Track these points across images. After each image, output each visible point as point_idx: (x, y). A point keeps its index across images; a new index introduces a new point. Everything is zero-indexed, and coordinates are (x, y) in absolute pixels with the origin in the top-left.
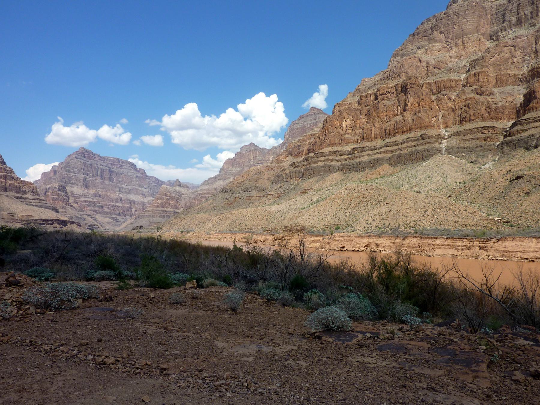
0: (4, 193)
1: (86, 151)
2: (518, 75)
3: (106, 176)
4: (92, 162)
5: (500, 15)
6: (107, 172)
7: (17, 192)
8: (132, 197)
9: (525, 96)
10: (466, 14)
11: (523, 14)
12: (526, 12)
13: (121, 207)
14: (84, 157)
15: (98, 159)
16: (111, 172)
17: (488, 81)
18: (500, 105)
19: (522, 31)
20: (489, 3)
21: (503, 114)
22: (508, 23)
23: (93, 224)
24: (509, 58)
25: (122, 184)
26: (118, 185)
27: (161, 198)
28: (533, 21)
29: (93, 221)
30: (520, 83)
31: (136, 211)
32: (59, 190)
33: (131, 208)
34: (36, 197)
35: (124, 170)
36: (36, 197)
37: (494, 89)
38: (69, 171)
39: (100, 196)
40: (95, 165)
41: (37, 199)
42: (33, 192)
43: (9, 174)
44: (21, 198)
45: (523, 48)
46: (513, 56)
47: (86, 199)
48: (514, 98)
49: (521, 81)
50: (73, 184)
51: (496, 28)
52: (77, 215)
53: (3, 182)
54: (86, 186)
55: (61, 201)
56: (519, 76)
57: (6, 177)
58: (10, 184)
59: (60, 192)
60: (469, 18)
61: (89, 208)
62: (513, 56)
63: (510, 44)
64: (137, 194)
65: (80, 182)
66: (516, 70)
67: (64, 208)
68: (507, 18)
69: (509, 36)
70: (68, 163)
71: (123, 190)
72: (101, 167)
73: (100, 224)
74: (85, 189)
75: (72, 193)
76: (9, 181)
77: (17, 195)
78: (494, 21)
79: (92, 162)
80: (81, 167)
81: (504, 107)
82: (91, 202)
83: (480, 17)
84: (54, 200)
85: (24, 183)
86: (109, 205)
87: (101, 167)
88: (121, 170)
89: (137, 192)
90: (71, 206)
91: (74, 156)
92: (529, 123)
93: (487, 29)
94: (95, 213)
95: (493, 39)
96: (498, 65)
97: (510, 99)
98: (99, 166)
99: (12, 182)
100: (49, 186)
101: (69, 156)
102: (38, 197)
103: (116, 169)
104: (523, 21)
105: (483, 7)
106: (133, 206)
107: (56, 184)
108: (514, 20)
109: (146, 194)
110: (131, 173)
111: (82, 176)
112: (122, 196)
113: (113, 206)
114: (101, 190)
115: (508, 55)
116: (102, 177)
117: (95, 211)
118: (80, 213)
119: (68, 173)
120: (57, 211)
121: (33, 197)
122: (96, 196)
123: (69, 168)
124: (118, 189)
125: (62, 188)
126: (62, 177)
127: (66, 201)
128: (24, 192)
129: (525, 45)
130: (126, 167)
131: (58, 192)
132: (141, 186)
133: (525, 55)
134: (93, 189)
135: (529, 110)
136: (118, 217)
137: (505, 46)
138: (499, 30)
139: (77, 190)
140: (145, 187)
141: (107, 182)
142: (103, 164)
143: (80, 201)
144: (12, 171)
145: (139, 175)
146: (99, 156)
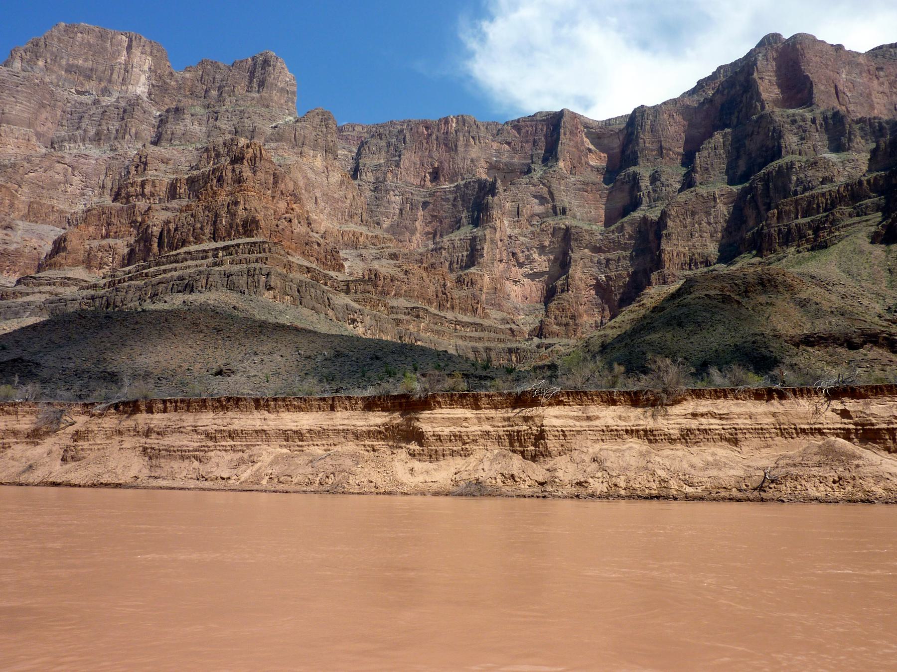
2: (66, 212)
5: (76, 116)
9: (55, 243)
10: (18, 91)
11: (105, 128)
12: (111, 127)
17: (12, 205)
18: (12, 247)
19: (94, 151)
20: (66, 93)
21: (13, 263)
22: (81, 132)
24: (60, 183)
28: (116, 143)
30: (67, 226)
37: (20, 223)
45: (86, 175)
46: (67, 182)
48: (42, 243)
49: (69, 223)
51: (63, 133)
56: (68, 215)
60: (20, 98)
62: (67, 182)
63: (67, 161)
66: (67, 204)
68: (83, 125)
69: (71, 150)
78: (65, 122)
81: (18, 253)
83: (43, 106)
92: (41, 284)
93: (50, 130)
95: (54, 148)
96: (38, 186)
97: (34, 242)
104: (103, 137)
105: (52, 94)
108: (92, 132)
115: (60, 178)
129: (90, 171)
133: (87, 186)
135: (51, 266)
137: (59, 162)
138: (67, 138)
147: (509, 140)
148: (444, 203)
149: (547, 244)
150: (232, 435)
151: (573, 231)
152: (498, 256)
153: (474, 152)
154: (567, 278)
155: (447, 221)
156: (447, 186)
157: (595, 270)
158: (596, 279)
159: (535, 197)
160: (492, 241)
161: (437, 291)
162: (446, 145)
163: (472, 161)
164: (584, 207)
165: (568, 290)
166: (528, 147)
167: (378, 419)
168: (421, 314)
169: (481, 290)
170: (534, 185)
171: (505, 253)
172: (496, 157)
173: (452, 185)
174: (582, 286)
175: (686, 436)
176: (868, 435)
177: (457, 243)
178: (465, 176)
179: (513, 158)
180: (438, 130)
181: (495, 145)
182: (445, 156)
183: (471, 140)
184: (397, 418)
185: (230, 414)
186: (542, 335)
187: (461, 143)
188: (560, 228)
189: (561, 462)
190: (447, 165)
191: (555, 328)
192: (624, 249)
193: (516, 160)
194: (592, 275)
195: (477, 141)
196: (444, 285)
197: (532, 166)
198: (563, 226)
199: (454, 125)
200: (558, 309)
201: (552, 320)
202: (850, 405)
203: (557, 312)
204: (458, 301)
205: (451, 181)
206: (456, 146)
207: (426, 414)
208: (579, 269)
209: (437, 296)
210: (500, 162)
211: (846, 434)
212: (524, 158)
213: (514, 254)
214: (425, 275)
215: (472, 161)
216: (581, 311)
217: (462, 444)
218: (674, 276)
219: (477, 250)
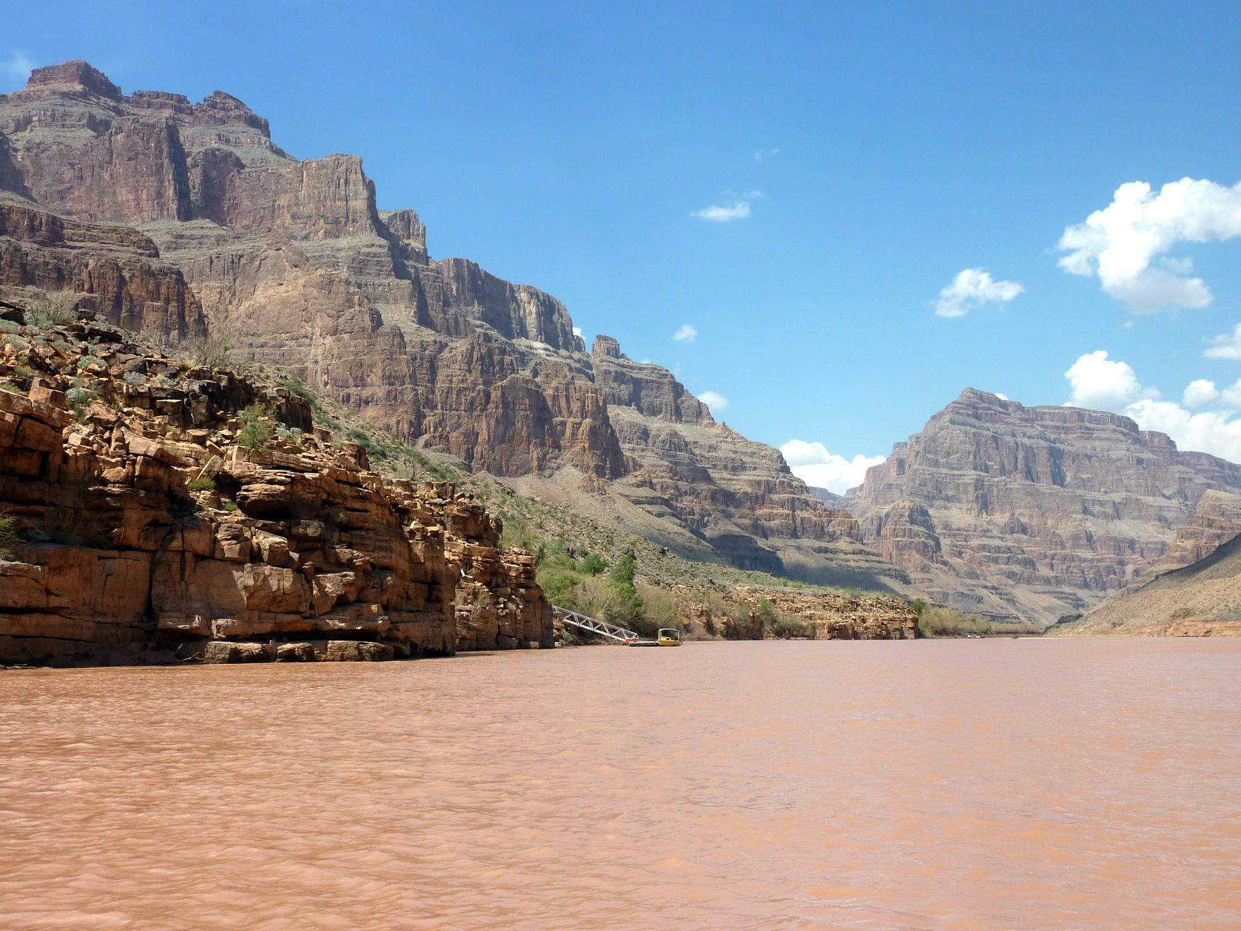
0: (792, 542)
1: (981, 397)
3: (1042, 466)
4: (1000, 427)
6: (1043, 457)
7: (817, 538)
8: (1125, 528)
13: (1091, 561)
14: (977, 417)
15: (1015, 418)
16: (1056, 455)
23: (1004, 612)
25: (1092, 488)
26: (1080, 492)
27: (1193, 535)
29: (1003, 603)
31: (1137, 572)
32: (913, 522)
33: (1122, 563)
34: (858, 546)
35: (1097, 443)
36: (858, 546)
38: (936, 464)
39: (1024, 530)
40: (1009, 439)
41: (861, 552)
42: (850, 535)
43: (799, 494)
44: (826, 550)
47: (986, 541)
50: (948, 499)
52: (961, 589)
53: (788, 515)
54: (985, 504)
55: (917, 551)
57: (793, 501)
58: (803, 519)
59: (915, 528)
61: (993, 567)
64: (1139, 517)
65: (966, 492)
67: (925, 569)
70: (933, 440)
71: (1096, 509)
72: (1026, 441)
73: (1025, 612)
74: (980, 512)
75: (947, 527)
76: (798, 512)
77: (818, 544)
79: (1000, 427)
80: (968, 447)
82: (998, 549)
84: (901, 548)
85: (830, 515)
86: (1053, 557)
87: (1026, 441)
88: (1089, 445)
89: (1141, 512)
90: (945, 563)
91: (947, 418)
94: (1011, 582)
98: (1019, 440)
99: (805, 514)
100: (887, 509)
101: (934, 418)
102: (863, 547)
103: (1072, 444)
106: (1128, 555)
107: (905, 504)
109: (1169, 515)
110: (1121, 451)
111: (971, 475)
112: (1095, 527)
113: (1064, 559)
114: (1026, 512)
116: (1030, 475)
117: (1011, 575)
118: (968, 581)
119: (934, 469)
120: (906, 581)
121: (850, 548)
122: (1012, 533)
123: (936, 453)
124: (1079, 507)
125: (919, 516)
126: (918, 482)
127: (931, 549)
128: (833, 537)
130: (1103, 435)
131: (908, 526)
132: (1154, 491)
134: (1003, 512)
136: (1082, 594)
139: (960, 515)
140: (1167, 492)
141: (1045, 486)
142: (1030, 431)
143: (967, 547)
144: (804, 488)
145: (1147, 455)
146: (1019, 407)
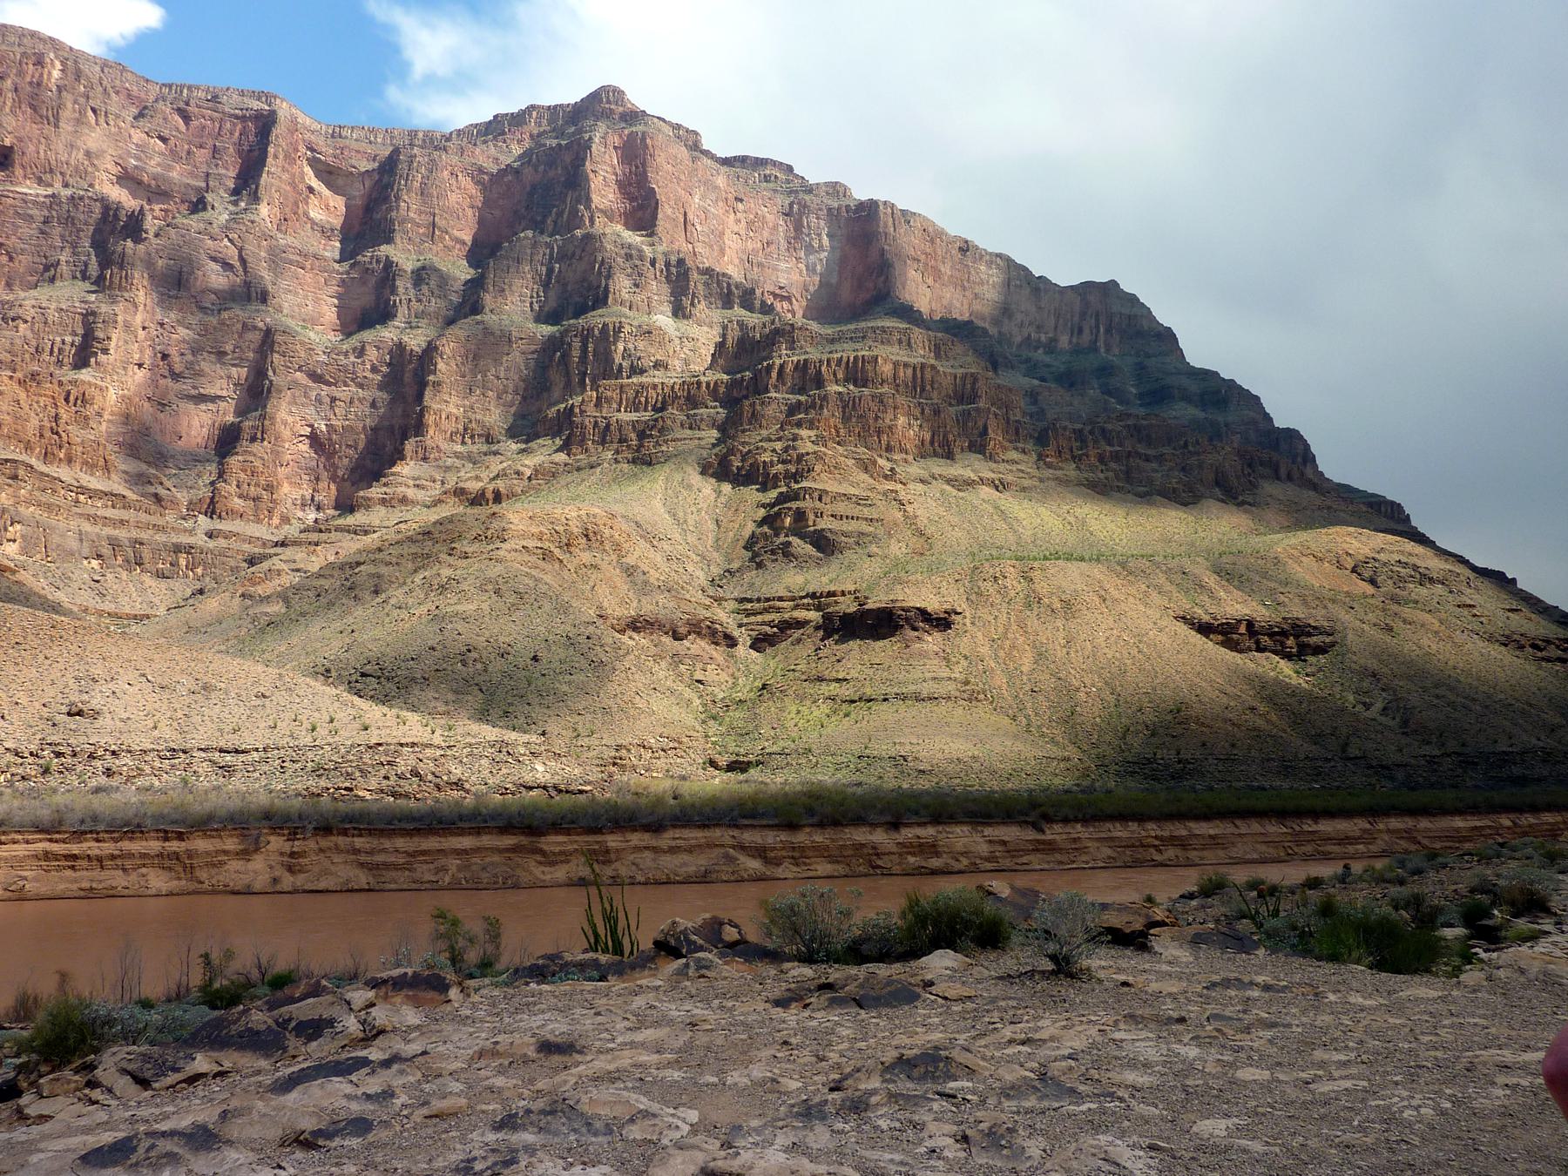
147: (166, 133)
148: (20, 222)
149: (229, 348)
150: (423, 853)
151: (279, 338)
152: (137, 356)
153: (94, 138)
154: (263, 417)
155: (23, 261)
156: (29, 189)
157: (310, 412)
158: (311, 426)
159: (214, 259)
160: (127, 326)
161: (41, 428)
162: (34, 108)
163: (88, 154)
164: (296, 293)
165: (263, 440)
166: (202, 155)
167: (509, 841)
168: (21, 472)
169: (99, 414)
170: (213, 238)
171: (148, 352)
172: (138, 158)
173: (42, 191)
174: (286, 433)
175: (673, 850)
176: (742, 848)
177: (53, 316)
178: (71, 181)
179: (170, 168)
180: (21, 73)
181: (138, 136)
182: (33, 129)
183: (90, 113)
184: (523, 840)
185: (416, 839)
186: (213, 512)
187: (67, 113)
188: (255, 328)
189: (617, 865)
190: (32, 148)
191: (237, 503)
192: (361, 386)
193: (174, 174)
194: (303, 418)
195: (102, 120)
196: (57, 418)
197: (209, 197)
198: (261, 325)
199: (56, 74)
200: (244, 471)
201: (233, 488)
202: (736, 833)
203: (242, 475)
204: (80, 449)
205: (40, 181)
206: (57, 118)
207: (543, 839)
208: (284, 405)
209: (41, 436)
210: (143, 169)
211: (733, 847)
212: (191, 174)
213: (165, 357)
214: (23, 396)
215: (88, 154)
216: (280, 476)
217: (564, 857)
218: (439, 450)
219: (95, 339)
